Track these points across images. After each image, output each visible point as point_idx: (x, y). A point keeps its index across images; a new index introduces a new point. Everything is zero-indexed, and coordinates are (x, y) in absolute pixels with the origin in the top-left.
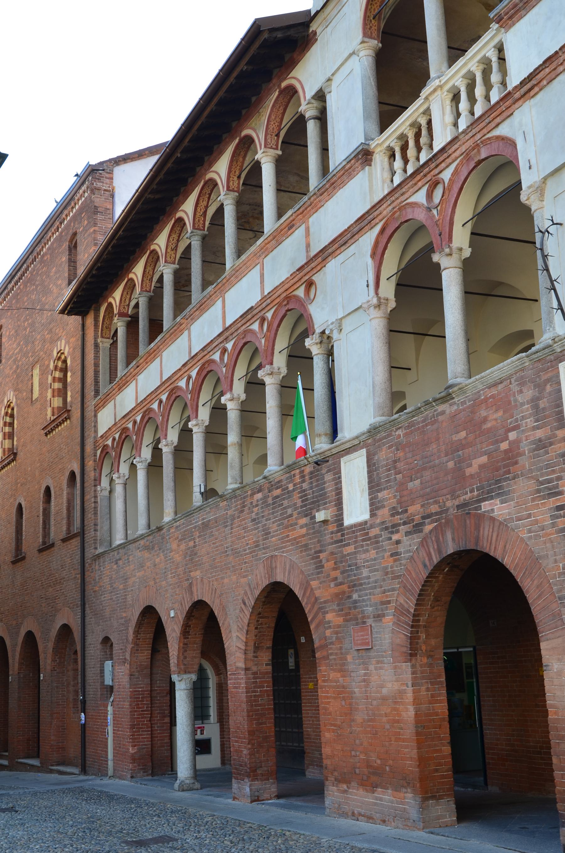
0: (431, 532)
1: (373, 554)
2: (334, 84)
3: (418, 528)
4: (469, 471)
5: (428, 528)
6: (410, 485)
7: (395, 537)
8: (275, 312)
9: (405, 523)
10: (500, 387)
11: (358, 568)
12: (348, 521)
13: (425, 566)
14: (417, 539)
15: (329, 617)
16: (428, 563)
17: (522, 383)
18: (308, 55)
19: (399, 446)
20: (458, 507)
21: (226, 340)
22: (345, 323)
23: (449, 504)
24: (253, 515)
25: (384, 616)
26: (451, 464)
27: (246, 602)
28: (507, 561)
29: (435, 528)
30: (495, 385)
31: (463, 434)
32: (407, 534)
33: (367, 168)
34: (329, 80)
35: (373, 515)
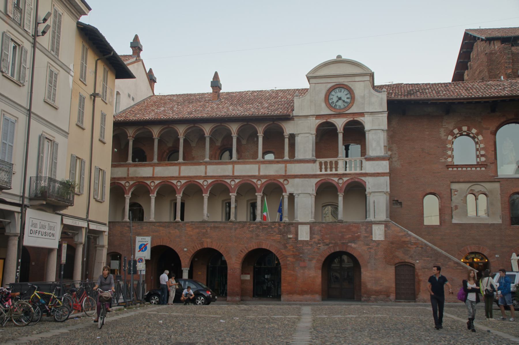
0: (332, 246)
1: (310, 247)
2: (299, 136)
3: (327, 245)
4: (345, 237)
5: (331, 245)
6: (326, 236)
7: (319, 245)
8: (267, 181)
9: (323, 243)
10: (357, 224)
11: (303, 250)
12: (299, 239)
13: (329, 252)
14: (326, 247)
15: (288, 259)
16: (330, 252)
17: (363, 225)
18: (289, 121)
19: (323, 227)
20: (341, 243)
21: (235, 179)
22: (300, 195)
23: (338, 242)
24: (250, 230)
25: (312, 260)
26: (340, 235)
27: (243, 251)
28: (354, 255)
29: (333, 246)
30: (355, 223)
31: (345, 230)
32: (323, 245)
33: (315, 164)
34: (299, 134)
35: (310, 239)
